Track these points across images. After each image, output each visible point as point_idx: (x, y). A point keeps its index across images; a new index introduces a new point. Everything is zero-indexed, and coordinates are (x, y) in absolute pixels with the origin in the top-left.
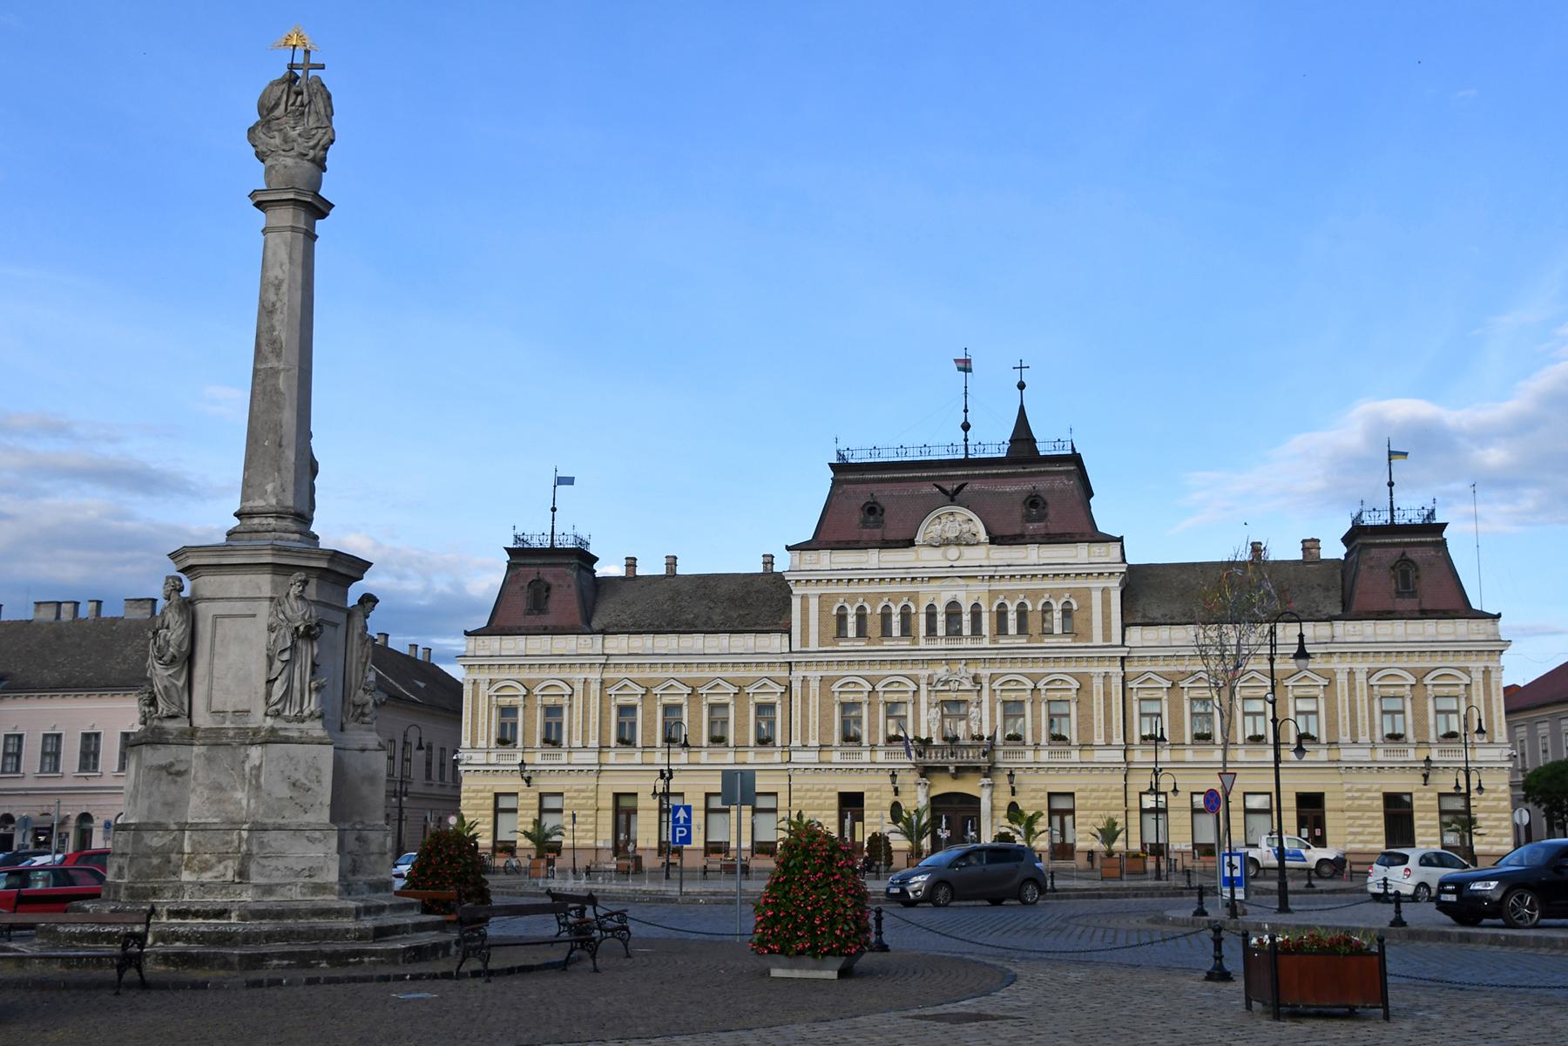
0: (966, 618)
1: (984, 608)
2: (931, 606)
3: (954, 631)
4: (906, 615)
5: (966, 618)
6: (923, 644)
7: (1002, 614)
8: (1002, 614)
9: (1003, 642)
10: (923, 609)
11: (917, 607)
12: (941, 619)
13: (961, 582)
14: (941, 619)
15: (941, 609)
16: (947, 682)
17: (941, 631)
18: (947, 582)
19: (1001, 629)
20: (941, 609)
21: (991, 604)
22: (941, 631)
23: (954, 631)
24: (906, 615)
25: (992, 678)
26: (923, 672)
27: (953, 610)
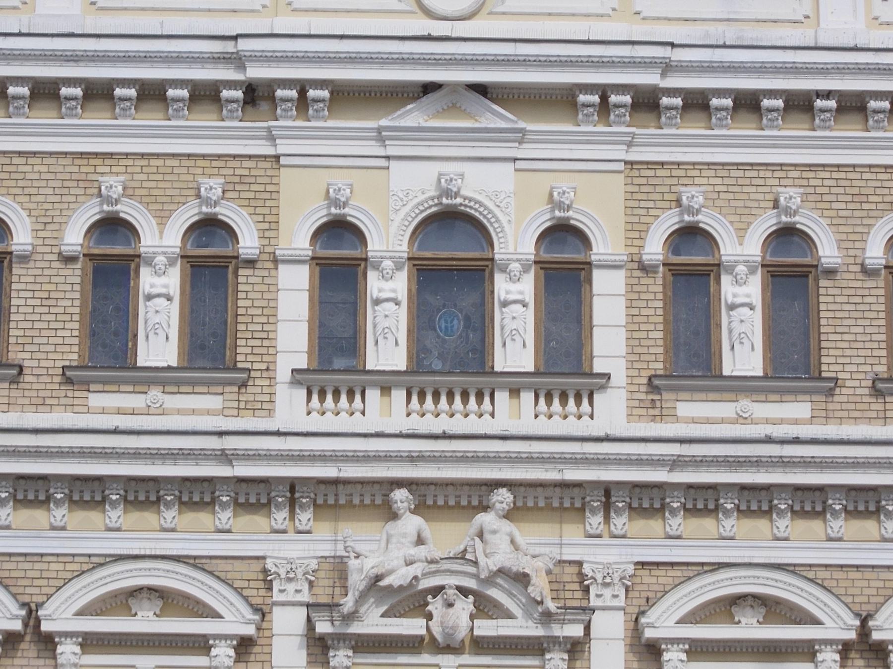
0: (515, 295)
1: (605, 244)
2: (338, 230)
3: (453, 355)
4: (212, 265)
5: (515, 295)
6: (291, 408)
7: (691, 272)
8: (691, 272)
9: (698, 414)
10: (298, 238)
11: (270, 226)
12: (388, 295)
13: (495, 117)
14: (388, 295)
15: (388, 238)
16: (414, 600)
17: (387, 346)
18: (413, 116)
19: (689, 357)
20: (388, 238)
21: (637, 231)
22: (387, 346)
23: (453, 355)
24: (212, 265)
25: (649, 580)
26: (295, 546)
27: (453, 257)
